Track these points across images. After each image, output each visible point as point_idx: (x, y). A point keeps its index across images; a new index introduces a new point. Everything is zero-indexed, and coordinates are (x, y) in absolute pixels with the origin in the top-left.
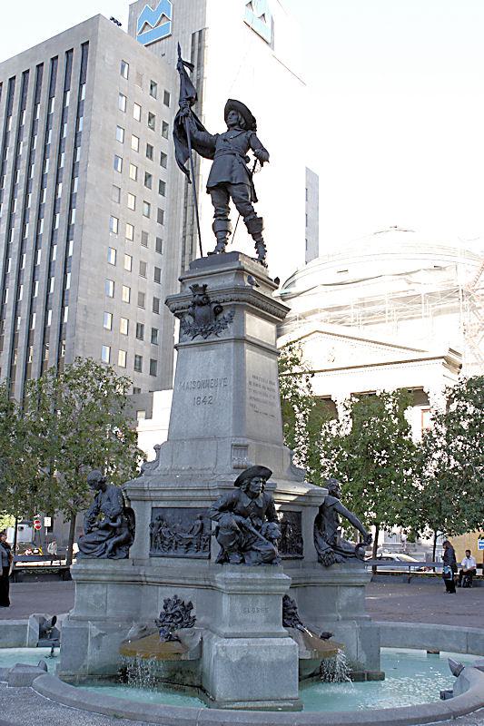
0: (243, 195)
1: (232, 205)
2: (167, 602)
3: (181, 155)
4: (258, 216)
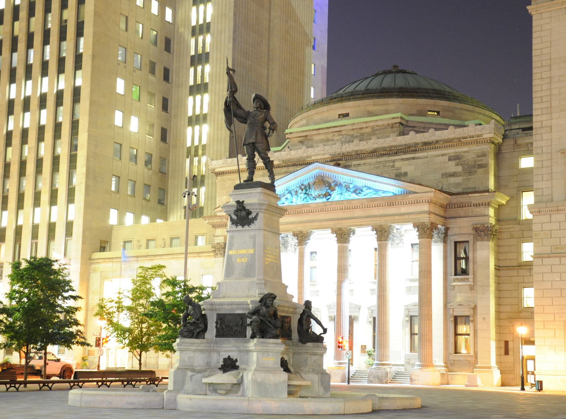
1: (256, 153)
2: (225, 360)
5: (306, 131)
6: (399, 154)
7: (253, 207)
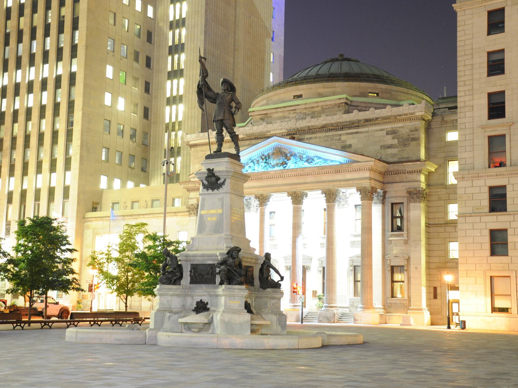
1: (224, 128)
2: (198, 303)
5: (266, 110)
6: (345, 129)
7: (221, 174)
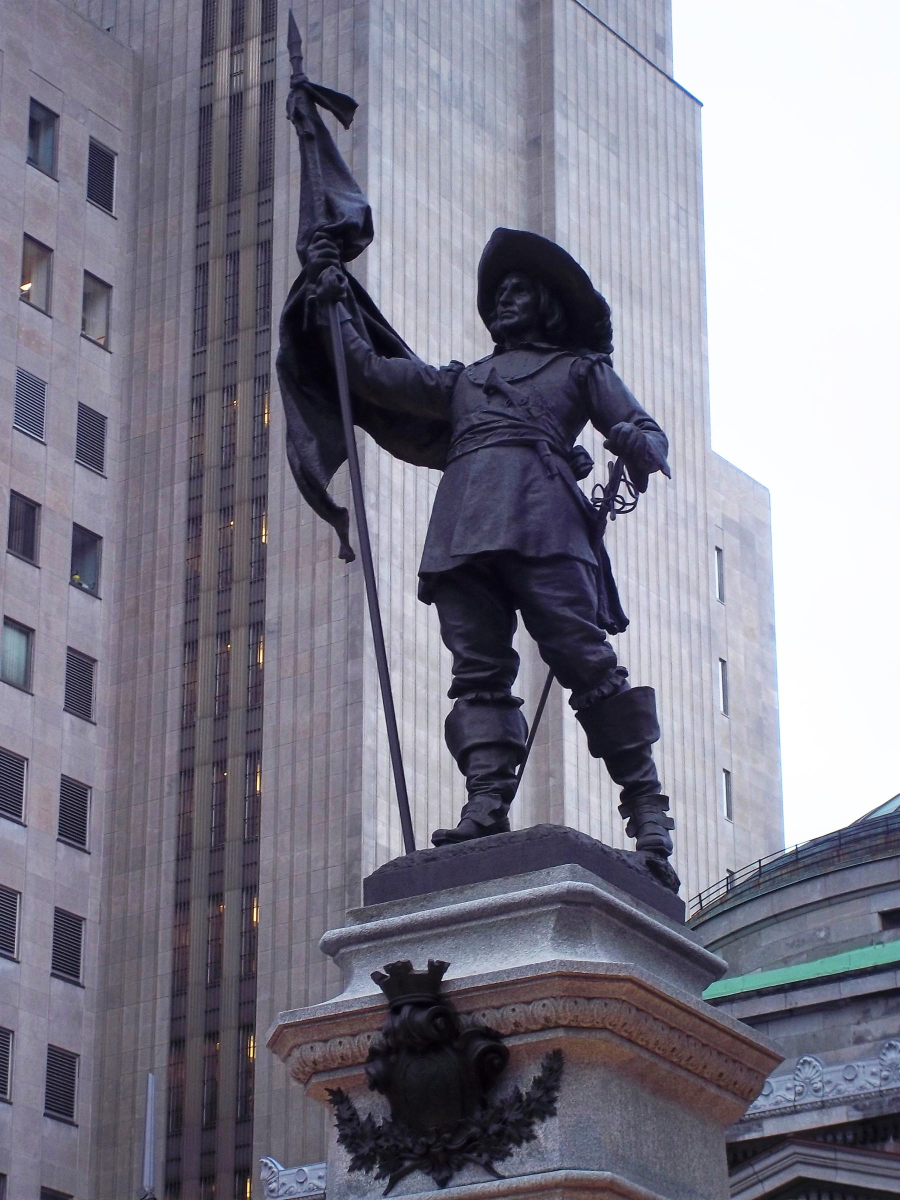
0: (570, 603)
3: (312, 449)
4: (633, 682)
7: (513, 1014)
